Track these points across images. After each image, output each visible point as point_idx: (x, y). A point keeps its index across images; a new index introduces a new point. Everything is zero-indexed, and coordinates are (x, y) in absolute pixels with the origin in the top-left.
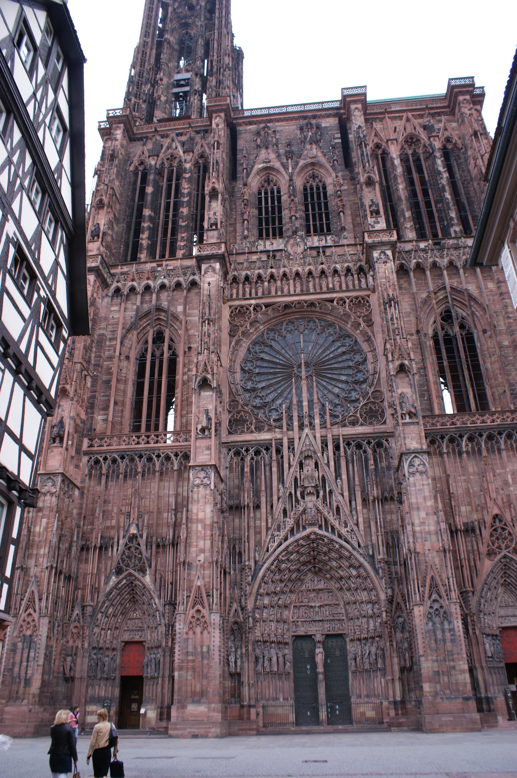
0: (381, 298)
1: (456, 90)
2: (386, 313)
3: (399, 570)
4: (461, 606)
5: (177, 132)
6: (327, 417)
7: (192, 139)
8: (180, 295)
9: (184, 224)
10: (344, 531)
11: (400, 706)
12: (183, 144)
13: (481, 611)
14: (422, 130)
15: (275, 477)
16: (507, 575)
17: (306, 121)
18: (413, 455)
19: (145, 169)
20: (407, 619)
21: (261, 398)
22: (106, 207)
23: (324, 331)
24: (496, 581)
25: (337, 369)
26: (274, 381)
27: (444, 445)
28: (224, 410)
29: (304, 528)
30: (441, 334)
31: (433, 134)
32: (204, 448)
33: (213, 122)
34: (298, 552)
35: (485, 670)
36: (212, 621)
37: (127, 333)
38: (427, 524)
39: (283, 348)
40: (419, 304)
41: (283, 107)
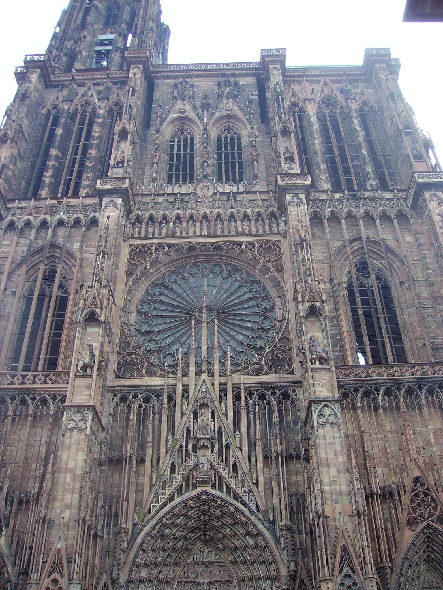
0: (293, 240)
1: (372, 58)
2: (297, 255)
3: (304, 539)
4: (378, 584)
5: (94, 81)
6: (229, 363)
7: (108, 88)
8: (78, 232)
9: (90, 165)
10: (240, 491)
12: (99, 93)
14: (340, 93)
15: (164, 427)
16: (430, 549)
17: (224, 79)
18: (323, 404)
19: (58, 113)
21: (157, 342)
22: (9, 141)
24: (418, 556)
26: (173, 324)
27: (358, 399)
28: (113, 351)
29: (195, 487)
30: (355, 284)
31: (350, 97)
32: (84, 388)
33: (131, 72)
34: (185, 515)
37: (16, 268)
39: (185, 292)
40: (333, 252)
41: (203, 64)
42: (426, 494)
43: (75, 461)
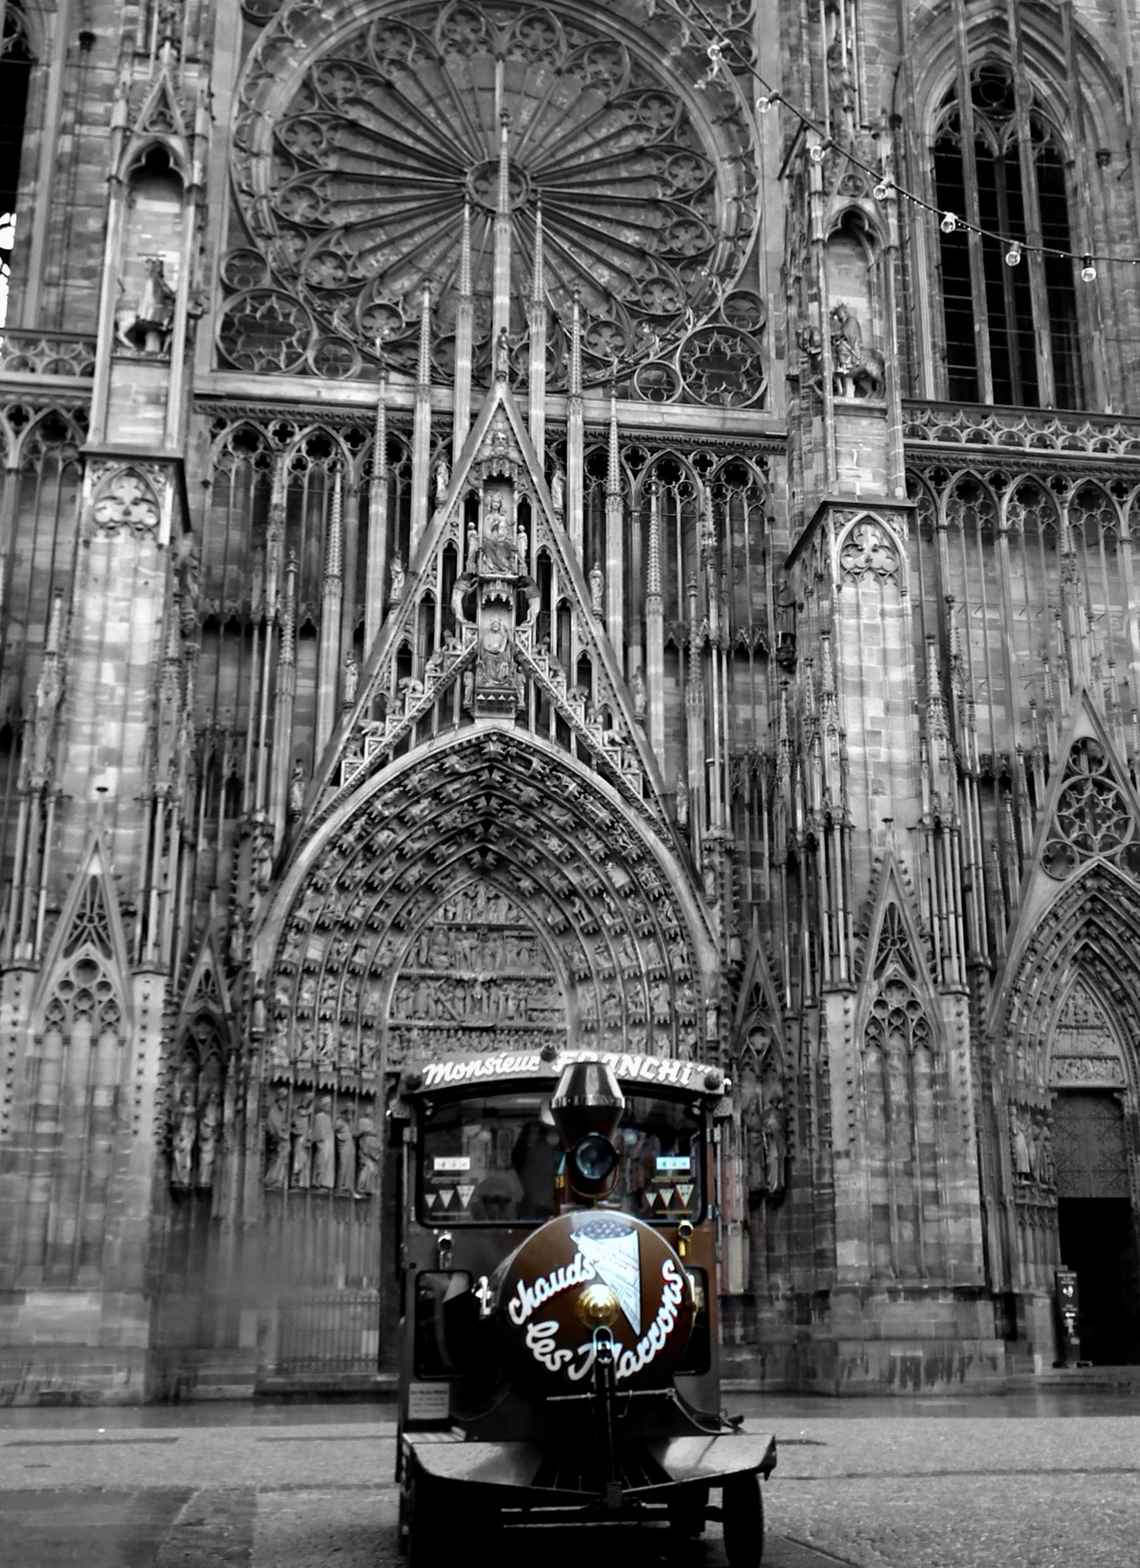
3: (765, 881)
10: (599, 739)
11: (738, 1314)
13: (1009, 1034)
15: (378, 535)
16: (1094, 930)
20: (780, 1039)
21: (341, 262)
23: (580, 67)
24: (1061, 945)
25: (611, 202)
26: (390, 209)
27: (943, 503)
29: (467, 717)
32: (142, 399)
34: (435, 795)
35: (1011, 1215)
36: (138, 1001)
38: (884, 737)
39: (431, 101)
42: (1101, 787)
43: (126, 625)
